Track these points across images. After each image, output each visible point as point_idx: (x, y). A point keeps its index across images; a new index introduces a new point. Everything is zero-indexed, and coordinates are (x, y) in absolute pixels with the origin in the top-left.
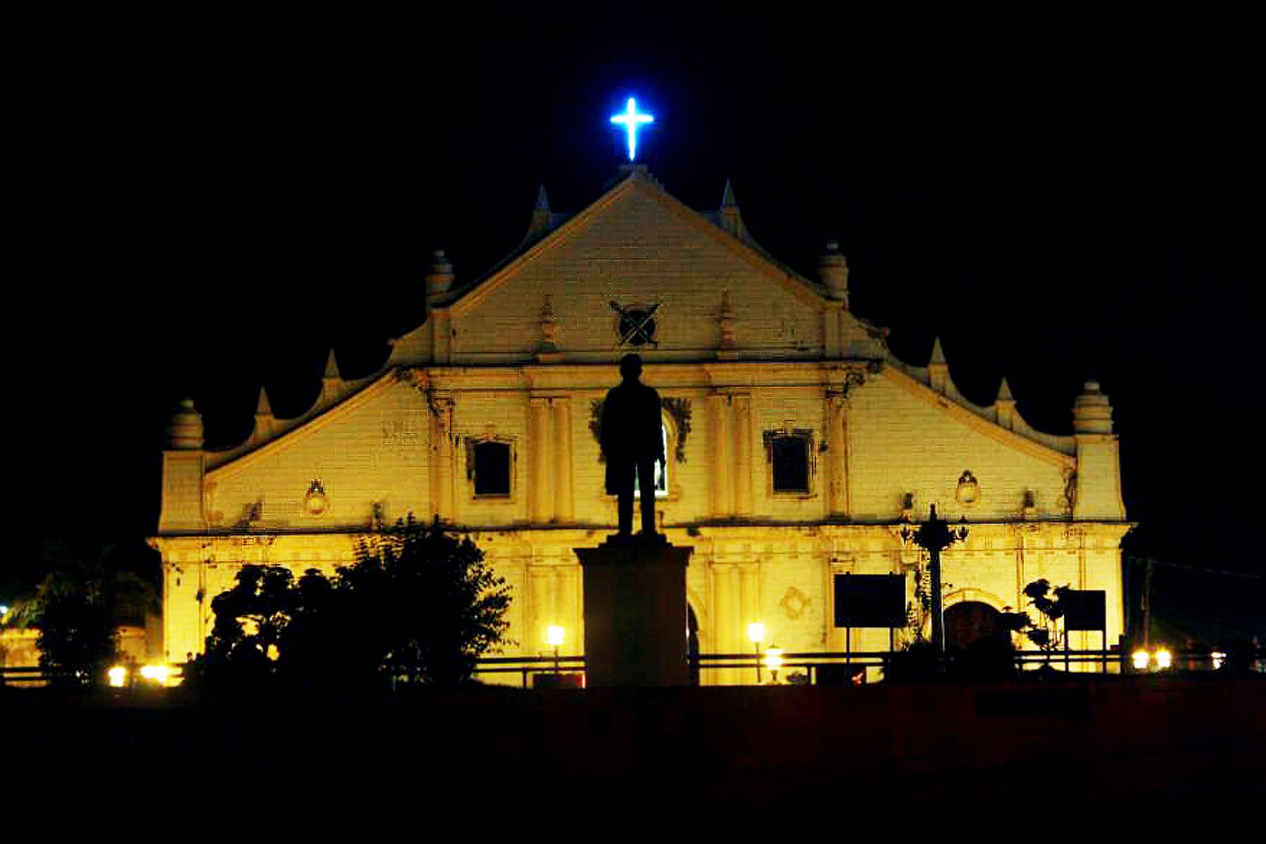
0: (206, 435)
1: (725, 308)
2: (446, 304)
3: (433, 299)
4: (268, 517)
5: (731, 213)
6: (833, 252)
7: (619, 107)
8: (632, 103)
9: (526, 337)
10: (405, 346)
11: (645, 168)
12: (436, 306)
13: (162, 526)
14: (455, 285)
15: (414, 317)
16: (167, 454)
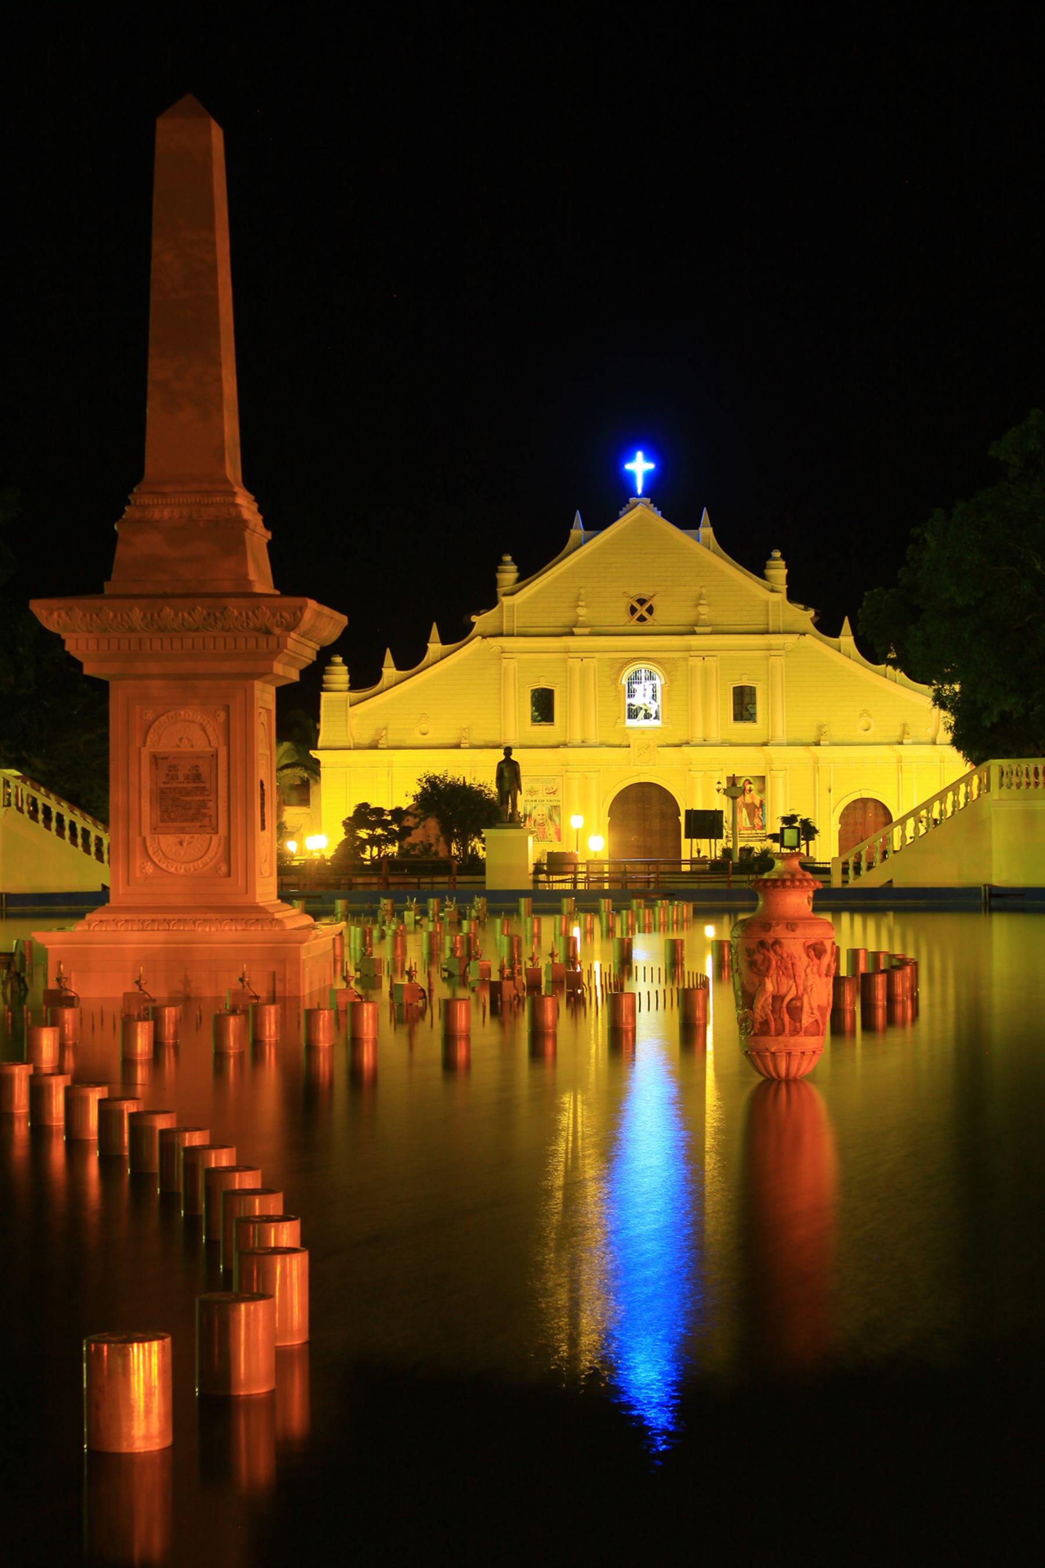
0: (351, 681)
1: (700, 597)
2: (512, 594)
3: (500, 590)
4: (392, 738)
5: (706, 531)
6: (775, 559)
7: (630, 458)
8: (640, 455)
9: (564, 618)
10: (481, 621)
11: (648, 500)
12: (505, 595)
13: (320, 744)
14: (519, 580)
15: (490, 601)
16: (322, 693)
